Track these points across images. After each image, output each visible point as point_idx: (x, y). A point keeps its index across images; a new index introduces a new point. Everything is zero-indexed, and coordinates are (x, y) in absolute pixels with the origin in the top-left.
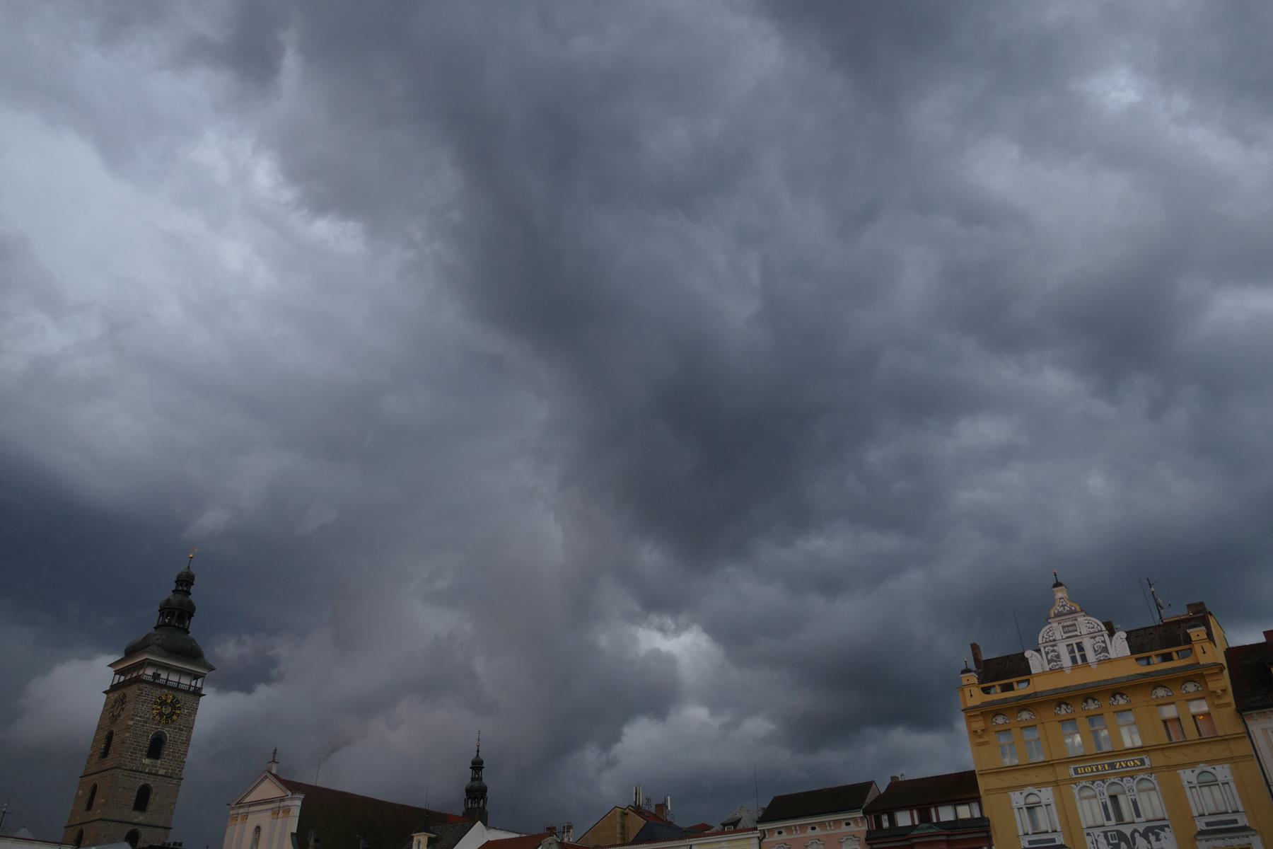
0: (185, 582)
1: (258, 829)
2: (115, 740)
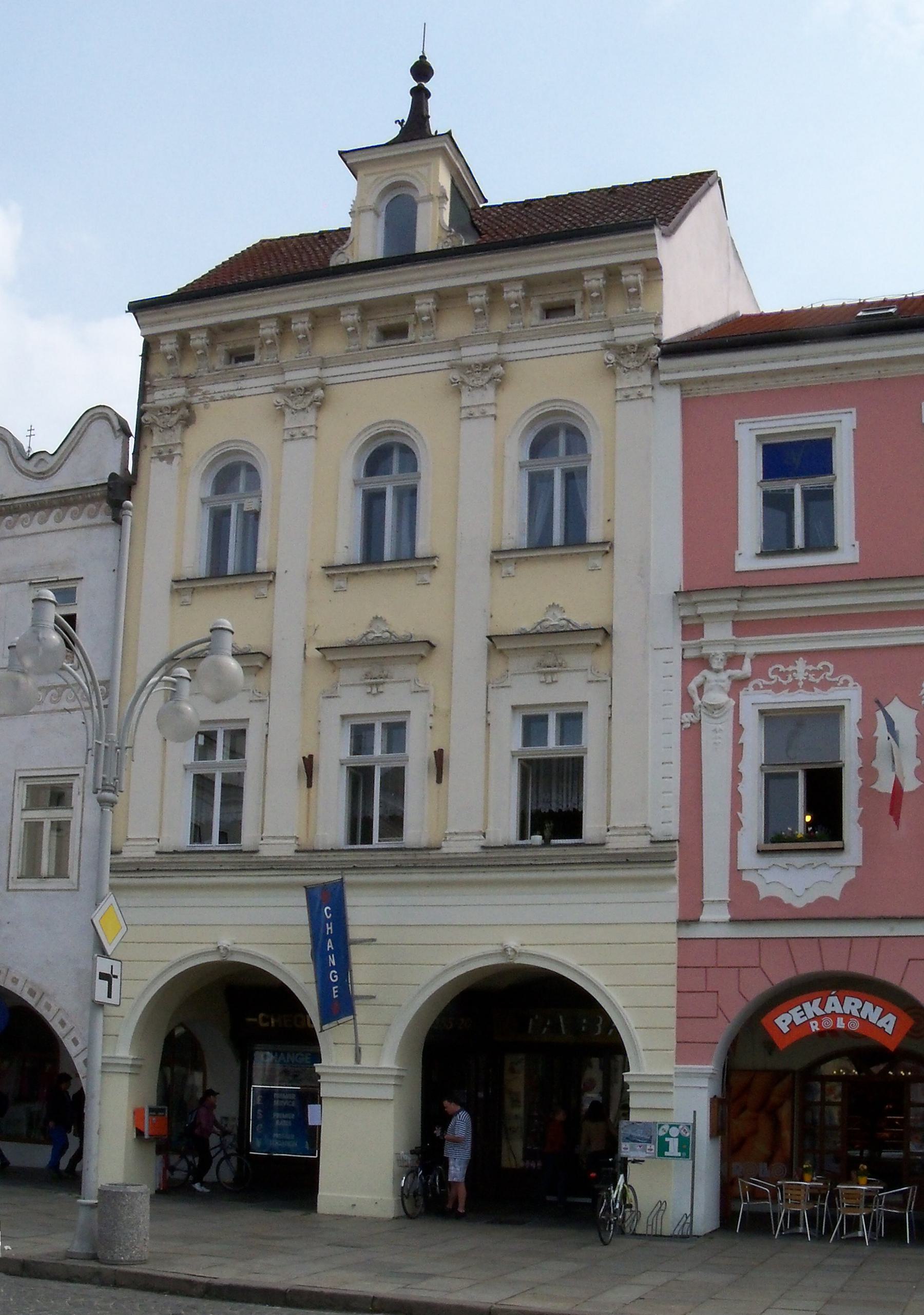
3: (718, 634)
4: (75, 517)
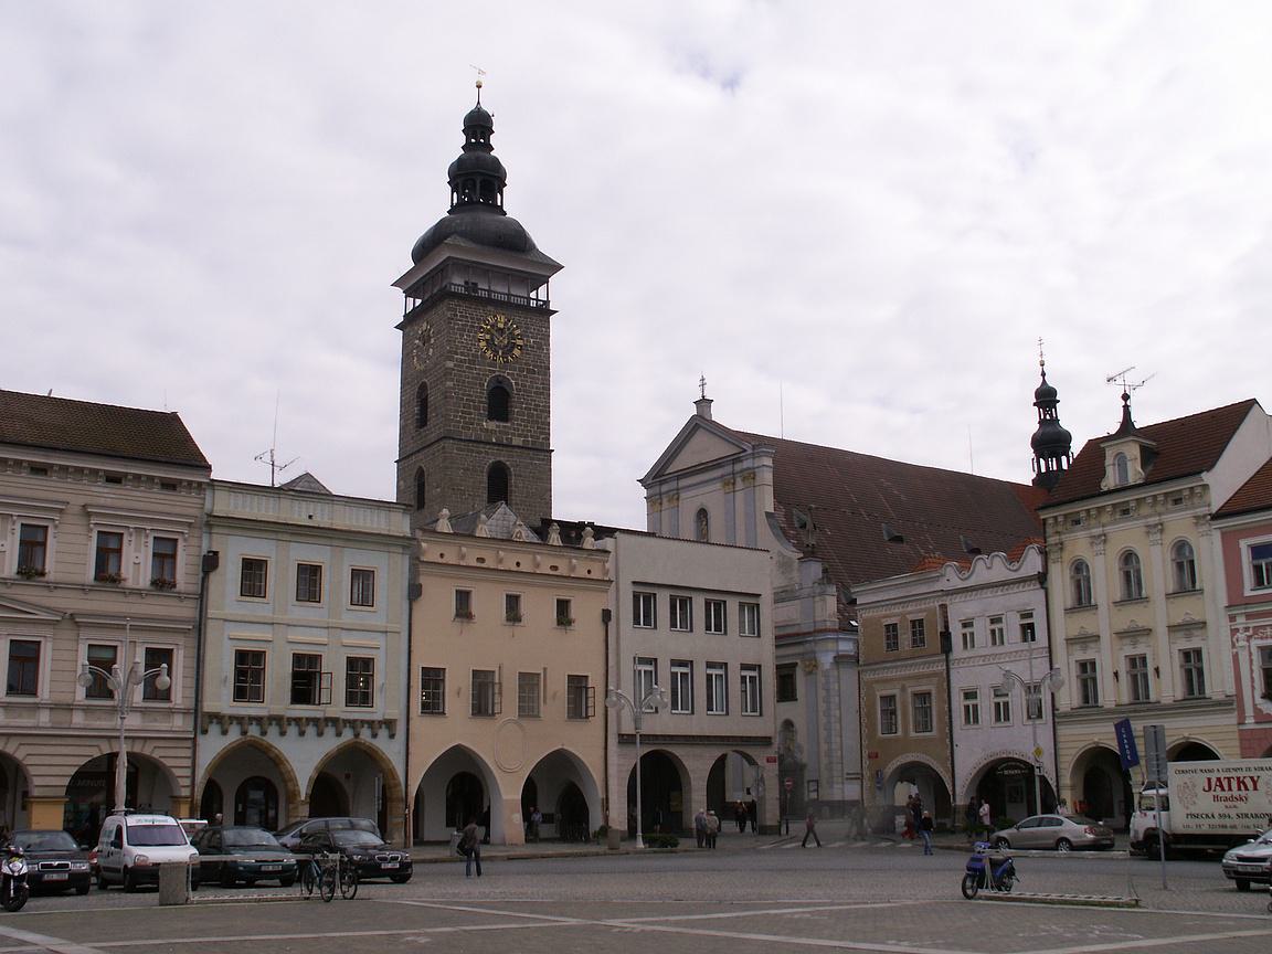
0: (478, 126)
1: (702, 514)
2: (434, 398)
3: (1241, 620)
4: (1029, 586)
